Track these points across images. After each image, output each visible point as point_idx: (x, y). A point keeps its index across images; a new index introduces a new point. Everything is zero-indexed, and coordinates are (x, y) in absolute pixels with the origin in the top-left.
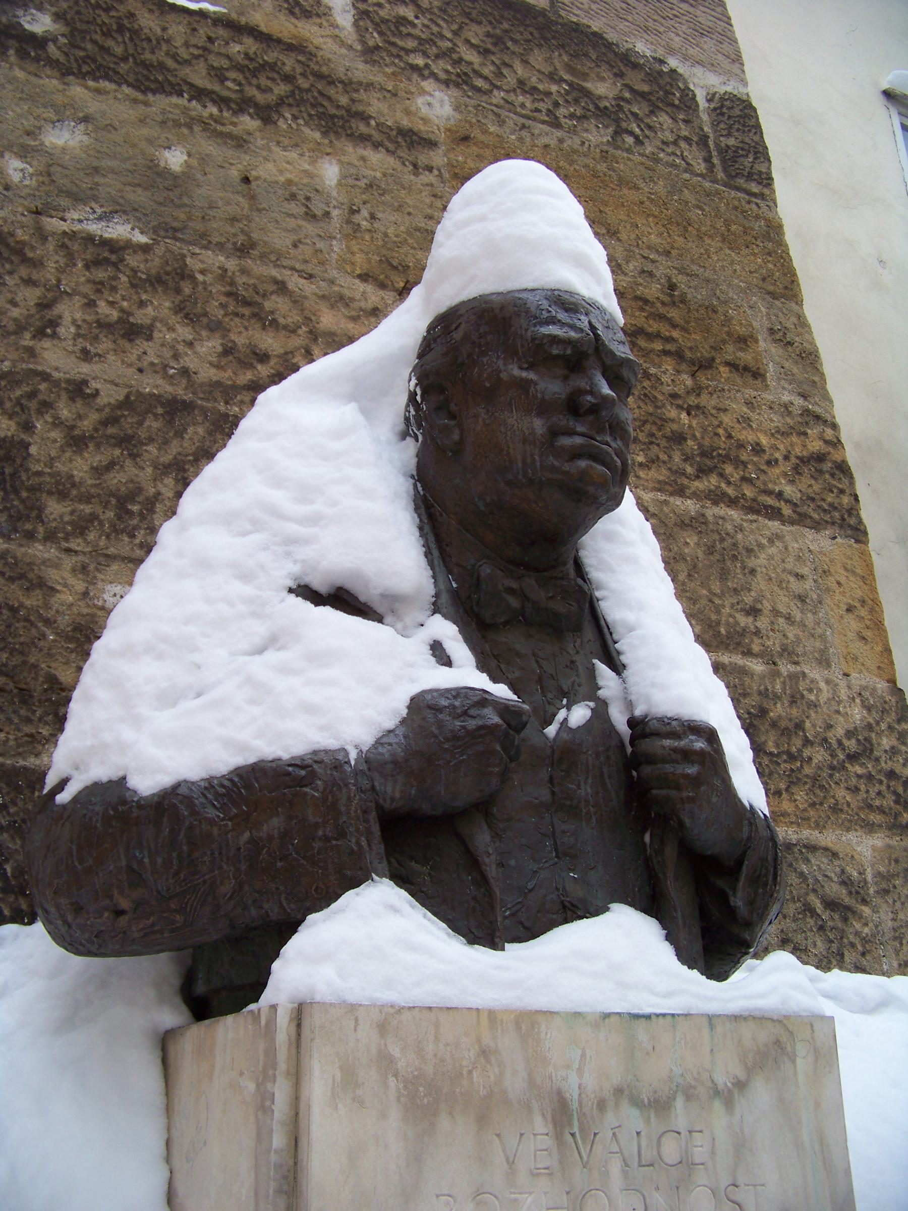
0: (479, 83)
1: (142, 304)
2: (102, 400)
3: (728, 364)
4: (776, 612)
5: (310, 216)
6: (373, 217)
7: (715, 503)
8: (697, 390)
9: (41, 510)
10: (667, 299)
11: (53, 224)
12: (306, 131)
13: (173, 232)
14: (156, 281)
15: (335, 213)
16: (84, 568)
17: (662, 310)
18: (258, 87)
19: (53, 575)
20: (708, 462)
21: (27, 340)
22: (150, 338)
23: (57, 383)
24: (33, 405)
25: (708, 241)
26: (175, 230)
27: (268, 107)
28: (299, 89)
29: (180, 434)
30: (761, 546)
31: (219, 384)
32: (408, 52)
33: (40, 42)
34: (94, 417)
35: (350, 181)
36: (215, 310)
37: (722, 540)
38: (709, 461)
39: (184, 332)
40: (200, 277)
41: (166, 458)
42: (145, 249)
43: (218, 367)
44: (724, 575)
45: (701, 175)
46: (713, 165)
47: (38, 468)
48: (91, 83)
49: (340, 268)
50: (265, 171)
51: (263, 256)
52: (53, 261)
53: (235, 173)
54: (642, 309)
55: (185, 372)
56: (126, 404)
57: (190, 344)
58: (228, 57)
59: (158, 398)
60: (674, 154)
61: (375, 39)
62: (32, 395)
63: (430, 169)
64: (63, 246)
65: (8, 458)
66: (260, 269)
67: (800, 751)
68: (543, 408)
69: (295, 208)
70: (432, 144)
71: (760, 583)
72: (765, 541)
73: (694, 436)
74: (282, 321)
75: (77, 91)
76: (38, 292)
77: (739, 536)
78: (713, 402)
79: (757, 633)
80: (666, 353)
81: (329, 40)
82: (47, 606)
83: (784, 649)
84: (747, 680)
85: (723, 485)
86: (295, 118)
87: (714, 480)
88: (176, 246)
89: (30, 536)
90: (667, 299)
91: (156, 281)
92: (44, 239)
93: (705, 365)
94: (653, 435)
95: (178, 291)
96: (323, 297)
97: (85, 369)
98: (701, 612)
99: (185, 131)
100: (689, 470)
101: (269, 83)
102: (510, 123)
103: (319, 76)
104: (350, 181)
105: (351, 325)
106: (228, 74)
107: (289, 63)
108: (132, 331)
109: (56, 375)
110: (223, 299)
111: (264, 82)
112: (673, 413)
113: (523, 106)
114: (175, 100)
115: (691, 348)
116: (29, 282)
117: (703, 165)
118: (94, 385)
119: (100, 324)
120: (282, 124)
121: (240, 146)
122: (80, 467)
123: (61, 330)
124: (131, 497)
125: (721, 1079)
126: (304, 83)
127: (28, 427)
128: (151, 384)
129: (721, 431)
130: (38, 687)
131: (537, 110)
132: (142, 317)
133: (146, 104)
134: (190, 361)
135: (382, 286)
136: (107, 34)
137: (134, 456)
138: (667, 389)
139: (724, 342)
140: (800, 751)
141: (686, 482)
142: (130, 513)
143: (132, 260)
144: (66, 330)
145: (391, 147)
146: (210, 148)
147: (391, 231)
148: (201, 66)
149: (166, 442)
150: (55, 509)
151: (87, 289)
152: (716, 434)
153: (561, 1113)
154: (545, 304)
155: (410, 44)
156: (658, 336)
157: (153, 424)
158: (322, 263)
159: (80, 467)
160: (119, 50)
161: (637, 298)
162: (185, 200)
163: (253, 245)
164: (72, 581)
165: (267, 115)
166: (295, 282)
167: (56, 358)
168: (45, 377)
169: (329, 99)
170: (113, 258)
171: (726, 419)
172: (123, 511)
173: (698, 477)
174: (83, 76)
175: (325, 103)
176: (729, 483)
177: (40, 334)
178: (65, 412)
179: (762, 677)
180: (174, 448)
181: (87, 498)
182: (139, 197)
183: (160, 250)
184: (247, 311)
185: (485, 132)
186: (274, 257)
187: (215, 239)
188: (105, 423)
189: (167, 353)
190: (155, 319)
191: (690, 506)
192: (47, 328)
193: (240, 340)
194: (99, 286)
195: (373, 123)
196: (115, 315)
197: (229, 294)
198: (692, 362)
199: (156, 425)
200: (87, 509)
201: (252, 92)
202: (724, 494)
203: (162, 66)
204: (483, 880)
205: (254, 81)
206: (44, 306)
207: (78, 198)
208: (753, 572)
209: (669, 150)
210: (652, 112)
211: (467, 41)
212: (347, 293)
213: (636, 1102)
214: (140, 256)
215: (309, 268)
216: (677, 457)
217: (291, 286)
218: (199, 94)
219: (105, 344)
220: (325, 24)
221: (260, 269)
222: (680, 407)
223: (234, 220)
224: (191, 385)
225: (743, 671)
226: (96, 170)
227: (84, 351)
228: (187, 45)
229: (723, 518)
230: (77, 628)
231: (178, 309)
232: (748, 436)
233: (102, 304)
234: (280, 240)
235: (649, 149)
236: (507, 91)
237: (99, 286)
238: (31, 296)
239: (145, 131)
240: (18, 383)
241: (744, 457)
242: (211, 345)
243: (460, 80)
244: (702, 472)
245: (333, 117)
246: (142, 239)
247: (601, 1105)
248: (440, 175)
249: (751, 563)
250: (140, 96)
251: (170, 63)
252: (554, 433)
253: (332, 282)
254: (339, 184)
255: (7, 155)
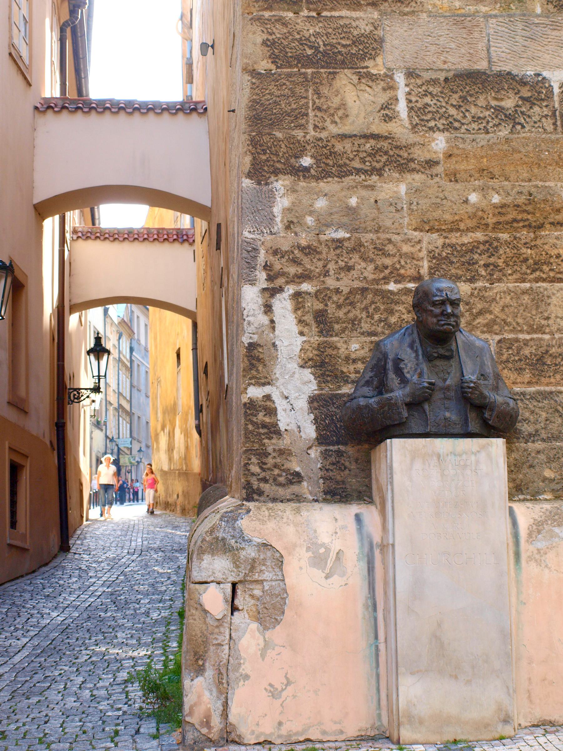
0: (456, 124)
1: (351, 259)
2: (344, 293)
3: (551, 223)
4: (557, 317)
5: (397, 211)
6: (418, 204)
7: (537, 282)
8: (536, 238)
9: (333, 328)
10: (527, 202)
11: (322, 237)
12: (394, 174)
13: (356, 230)
14: (354, 249)
15: (405, 206)
16: (346, 342)
17: (525, 208)
18: (377, 161)
19: (339, 345)
20: (537, 267)
21: (322, 278)
22: (354, 269)
23: (331, 290)
24: (327, 298)
25: (548, 167)
26: (357, 229)
27: (380, 169)
28: (390, 156)
29: (365, 298)
30: (554, 294)
31: (375, 279)
32: (428, 121)
33: (307, 170)
34: (343, 298)
35: (410, 191)
36: (372, 256)
37: (538, 295)
38: (537, 266)
39: (363, 264)
40: (366, 244)
41: (363, 306)
42: (349, 239)
43: (374, 274)
44: (538, 307)
45: (551, 133)
46: (557, 126)
47: (331, 316)
48: (325, 180)
49: (408, 229)
50: (382, 196)
51: (383, 232)
52: (325, 250)
53: (372, 200)
54: (516, 210)
55: (365, 278)
56: (350, 292)
57: (365, 269)
58: (366, 152)
59: (358, 288)
60: (539, 127)
61: (416, 120)
62: (326, 295)
63: (437, 175)
64: (327, 245)
65: (323, 315)
66: (383, 236)
67: (559, 363)
68: (436, 316)
69: (392, 209)
70: (437, 163)
71: (552, 307)
72: (556, 292)
73: (532, 258)
74: (391, 253)
75: (322, 184)
76: (322, 262)
77: (545, 293)
78: (542, 242)
79: (548, 326)
80: (524, 227)
81: (399, 128)
82: (338, 353)
83: (558, 329)
84: (542, 342)
85: (541, 274)
86: (390, 170)
87: (538, 273)
88: (357, 235)
89: (331, 336)
90: (527, 202)
91: (354, 249)
92: (321, 244)
93: (541, 227)
94: (515, 262)
95: (360, 251)
96: (403, 241)
97: (338, 283)
98: (527, 322)
99: (355, 189)
100: (529, 271)
101: (380, 158)
102: (468, 140)
103: (397, 147)
104: (410, 191)
105: (412, 249)
106: (367, 159)
107: (385, 145)
108: (349, 268)
109: (332, 287)
110: (373, 250)
111: (378, 158)
112: (524, 250)
113: (474, 129)
114: (351, 177)
115: (535, 221)
116: (319, 260)
117: (552, 127)
118: (341, 288)
119: (340, 268)
120: (386, 175)
121: (373, 190)
122: (341, 314)
123: (330, 273)
124: (355, 320)
125: (473, 451)
126: (391, 153)
127: (326, 305)
128: (357, 284)
129: (544, 253)
130: (339, 374)
131: (480, 129)
132: (351, 263)
133: (342, 182)
134: (366, 274)
135: (421, 231)
136: (327, 158)
137: (354, 308)
138: (523, 241)
139: (550, 214)
140: (559, 363)
141: (526, 276)
142: (355, 324)
143: (346, 244)
144: (332, 272)
145: (423, 170)
146: (364, 193)
147: (424, 207)
148: (357, 159)
149: (362, 302)
150: (337, 327)
151: (335, 258)
152: (542, 255)
153: (439, 456)
154: (435, 291)
155: (429, 116)
156: (522, 220)
157: (358, 297)
158: (402, 228)
159: (341, 314)
160: (331, 163)
161: (515, 206)
162: (359, 217)
163: (380, 228)
164: (343, 345)
165: (379, 172)
166: (395, 238)
167: (331, 282)
168: (328, 289)
169: (400, 156)
170: (341, 245)
171: (546, 247)
172: (353, 324)
173: (531, 274)
174: (322, 178)
175: (399, 159)
176: (544, 273)
177: (325, 276)
178: (335, 298)
179: (548, 340)
180: (365, 302)
181: (344, 322)
182: (345, 220)
183: (353, 238)
184: (380, 253)
185: (458, 148)
186: (386, 230)
187: (369, 229)
188: (346, 299)
189: (359, 273)
190: (355, 262)
191: (528, 285)
192: (326, 274)
193: (379, 263)
194: (338, 256)
195: (416, 162)
196: (343, 264)
197: (375, 248)
198: (535, 227)
199: (359, 297)
200: (344, 325)
201: (374, 164)
202: (542, 278)
203: (345, 165)
204: (426, 415)
205: (375, 159)
206: (324, 266)
207: (328, 226)
208: (549, 304)
209: (536, 125)
210: (531, 108)
211: (452, 105)
212: (410, 237)
213: (455, 455)
214: (348, 242)
215: (398, 231)
216: (524, 268)
217: (393, 240)
218: (358, 171)
219: (343, 274)
220: (397, 121)
221: (383, 236)
222: (527, 248)
223: (374, 220)
224: (367, 282)
225: (541, 339)
226: (331, 214)
227: (337, 278)
228: (352, 152)
229: (539, 287)
230: (346, 357)
231: (361, 257)
232: (554, 252)
233: (340, 261)
234: (388, 223)
235: (527, 128)
236: (467, 124)
237: (338, 256)
238: (320, 264)
239: (344, 193)
240: (322, 293)
241: (552, 260)
242: (371, 267)
243: (449, 127)
244: (534, 271)
245: (402, 164)
246: (348, 235)
247: (448, 455)
248: (441, 177)
249: (549, 301)
250: (340, 180)
251: (348, 162)
252: (438, 321)
253: (406, 234)
254: (406, 194)
255: (306, 216)
